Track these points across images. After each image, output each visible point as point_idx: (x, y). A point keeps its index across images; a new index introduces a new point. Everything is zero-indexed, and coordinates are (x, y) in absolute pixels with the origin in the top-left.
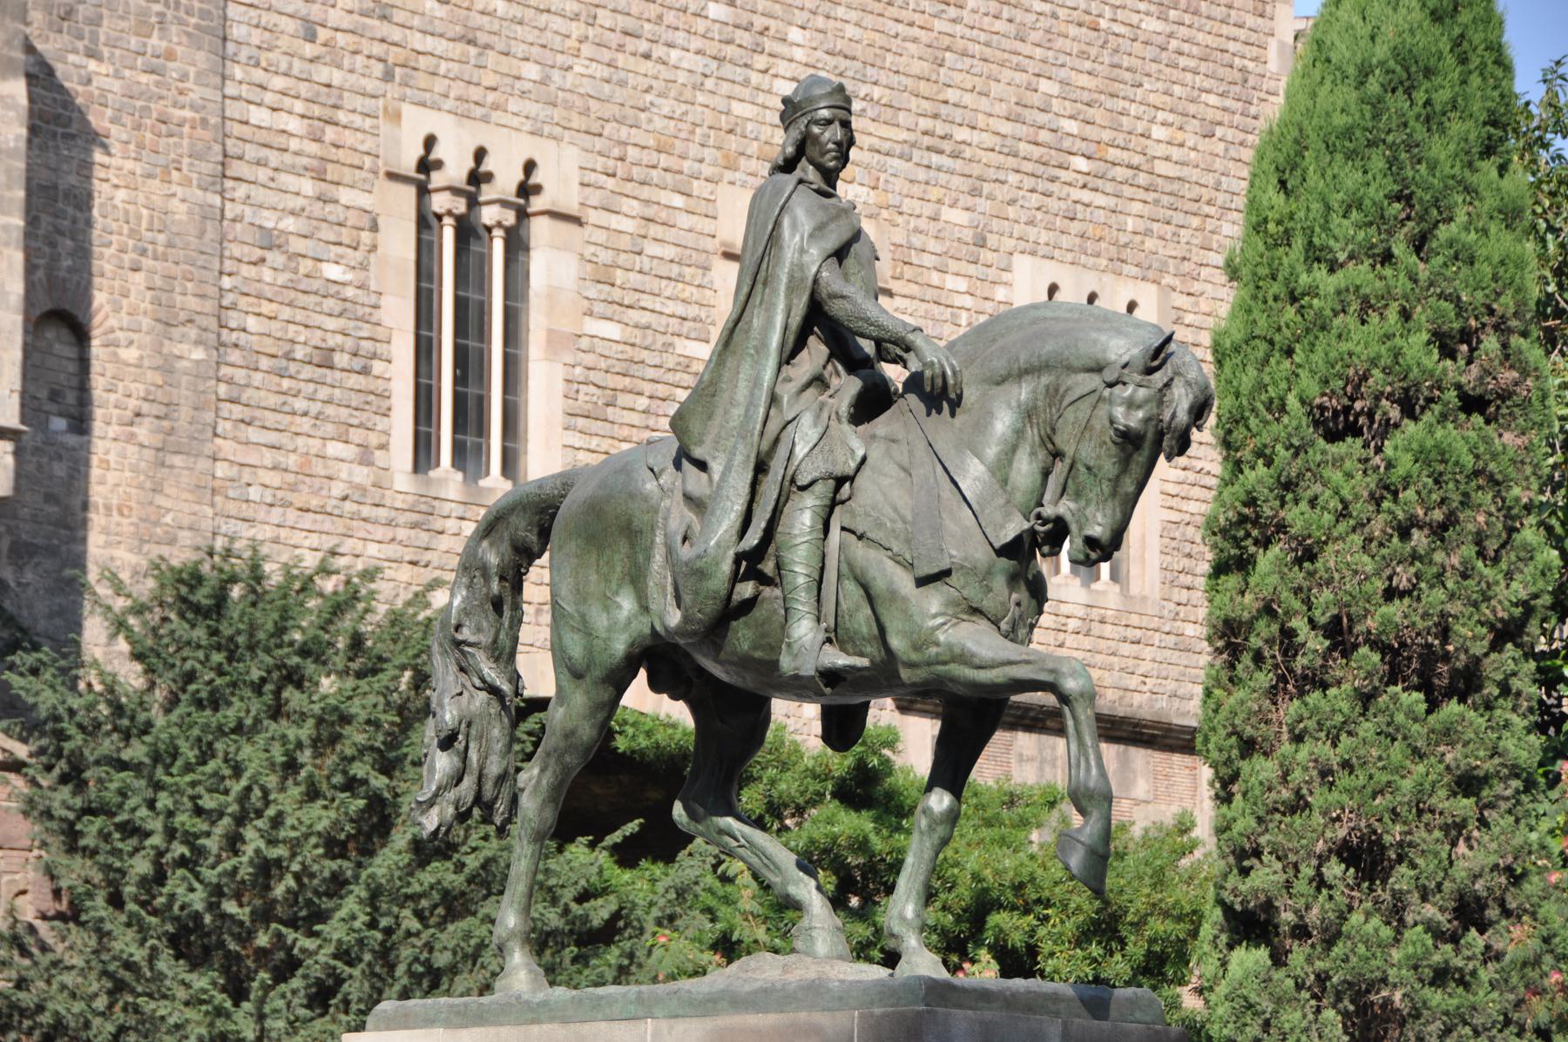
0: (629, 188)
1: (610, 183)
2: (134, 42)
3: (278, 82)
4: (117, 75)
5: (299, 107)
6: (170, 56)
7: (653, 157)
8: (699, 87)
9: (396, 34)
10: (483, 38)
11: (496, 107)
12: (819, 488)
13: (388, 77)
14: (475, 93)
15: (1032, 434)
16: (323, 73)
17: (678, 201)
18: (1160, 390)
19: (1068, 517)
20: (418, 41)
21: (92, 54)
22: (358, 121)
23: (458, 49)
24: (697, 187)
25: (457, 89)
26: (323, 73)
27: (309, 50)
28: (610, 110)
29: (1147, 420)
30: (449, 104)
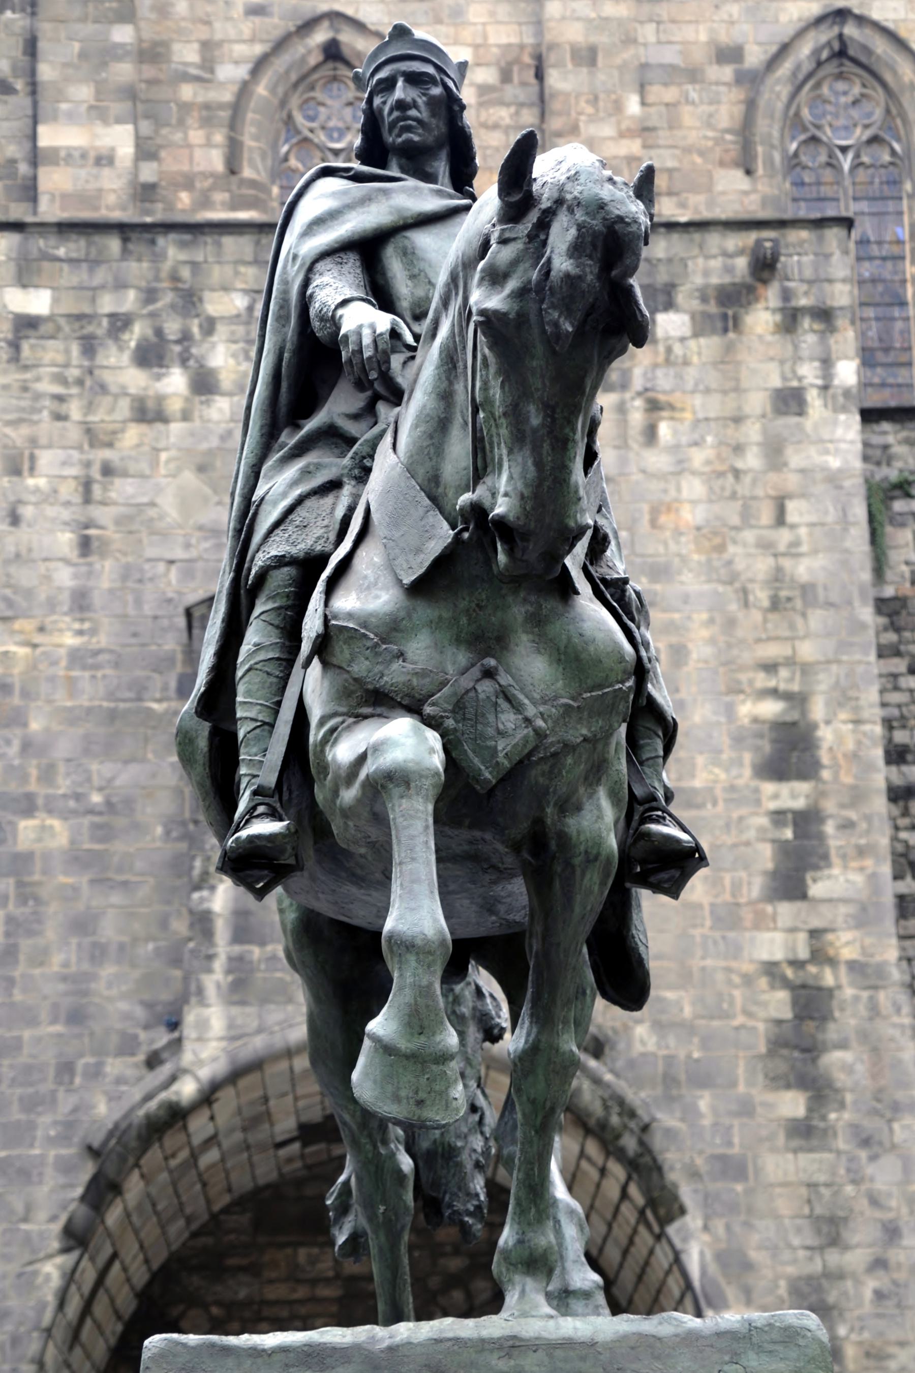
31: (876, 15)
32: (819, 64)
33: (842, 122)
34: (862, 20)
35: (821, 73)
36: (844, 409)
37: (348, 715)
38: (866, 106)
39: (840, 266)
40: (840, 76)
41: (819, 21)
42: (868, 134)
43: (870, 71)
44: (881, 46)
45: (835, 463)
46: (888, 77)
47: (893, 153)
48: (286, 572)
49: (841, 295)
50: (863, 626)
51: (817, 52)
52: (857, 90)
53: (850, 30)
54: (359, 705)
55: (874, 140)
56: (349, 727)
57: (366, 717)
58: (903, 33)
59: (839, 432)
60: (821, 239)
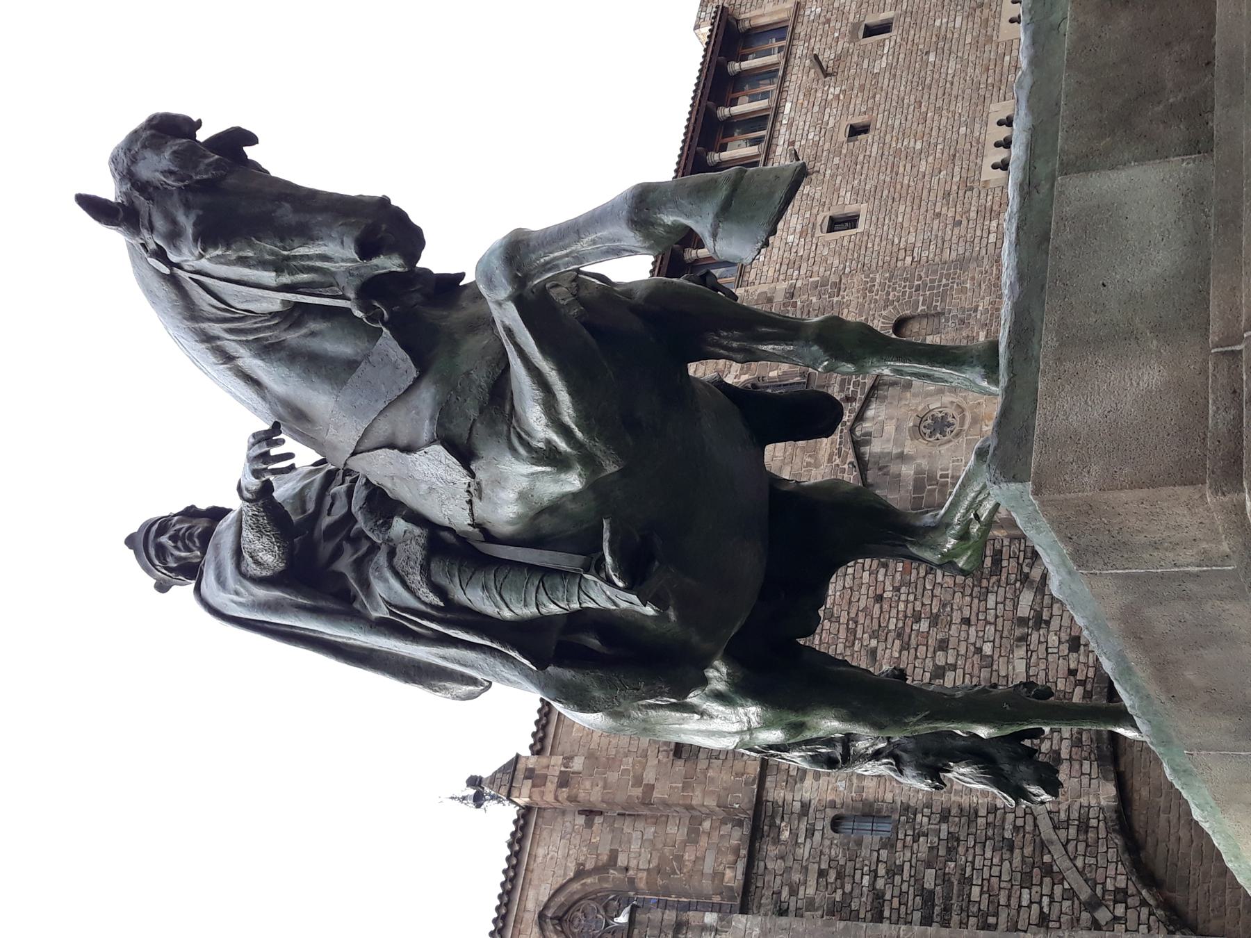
0: (1004, 81)
1: (1003, 88)
2: (970, 294)
3: (978, 233)
4: (983, 298)
5: (987, 223)
6: (973, 278)
7: (991, 72)
8: (962, 58)
9: (955, 188)
10: (952, 152)
11: (978, 142)
12: (442, 580)
13: (971, 189)
14: (974, 150)
15: (292, 337)
16: (973, 215)
17: (1007, 58)
18: (149, 198)
19: (357, 282)
20: (956, 179)
21: (976, 310)
22: (990, 197)
23: (958, 162)
24: (1001, 49)
25: (973, 157)
26: (973, 215)
27: (964, 222)
28: (975, 95)
29: (188, 207)
30: (979, 161)
31: (546, 899)
32: (563, 932)
33: (593, 925)
34: (546, 907)
35: (568, 932)
36: (729, 922)
37: (510, 425)
38: (589, 910)
39: (656, 915)
40: (571, 922)
41: (542, 929)
42: (602, 912)
43: (571, 906)
44: (561, 899)
45: (757, 931)
46: (576, 897)
47: (613, 899)
48: (434, 566)
49: (670, 916)
50: (846, 927)
51: (556, 932)
52: (579, 914)
53: (550, 914)
54: (503, 413)
55: (606, 908)
56: (517, 421)
57: (513, 407)
58: (557, 886)
59: (741, 926)
60: (641, 923)
